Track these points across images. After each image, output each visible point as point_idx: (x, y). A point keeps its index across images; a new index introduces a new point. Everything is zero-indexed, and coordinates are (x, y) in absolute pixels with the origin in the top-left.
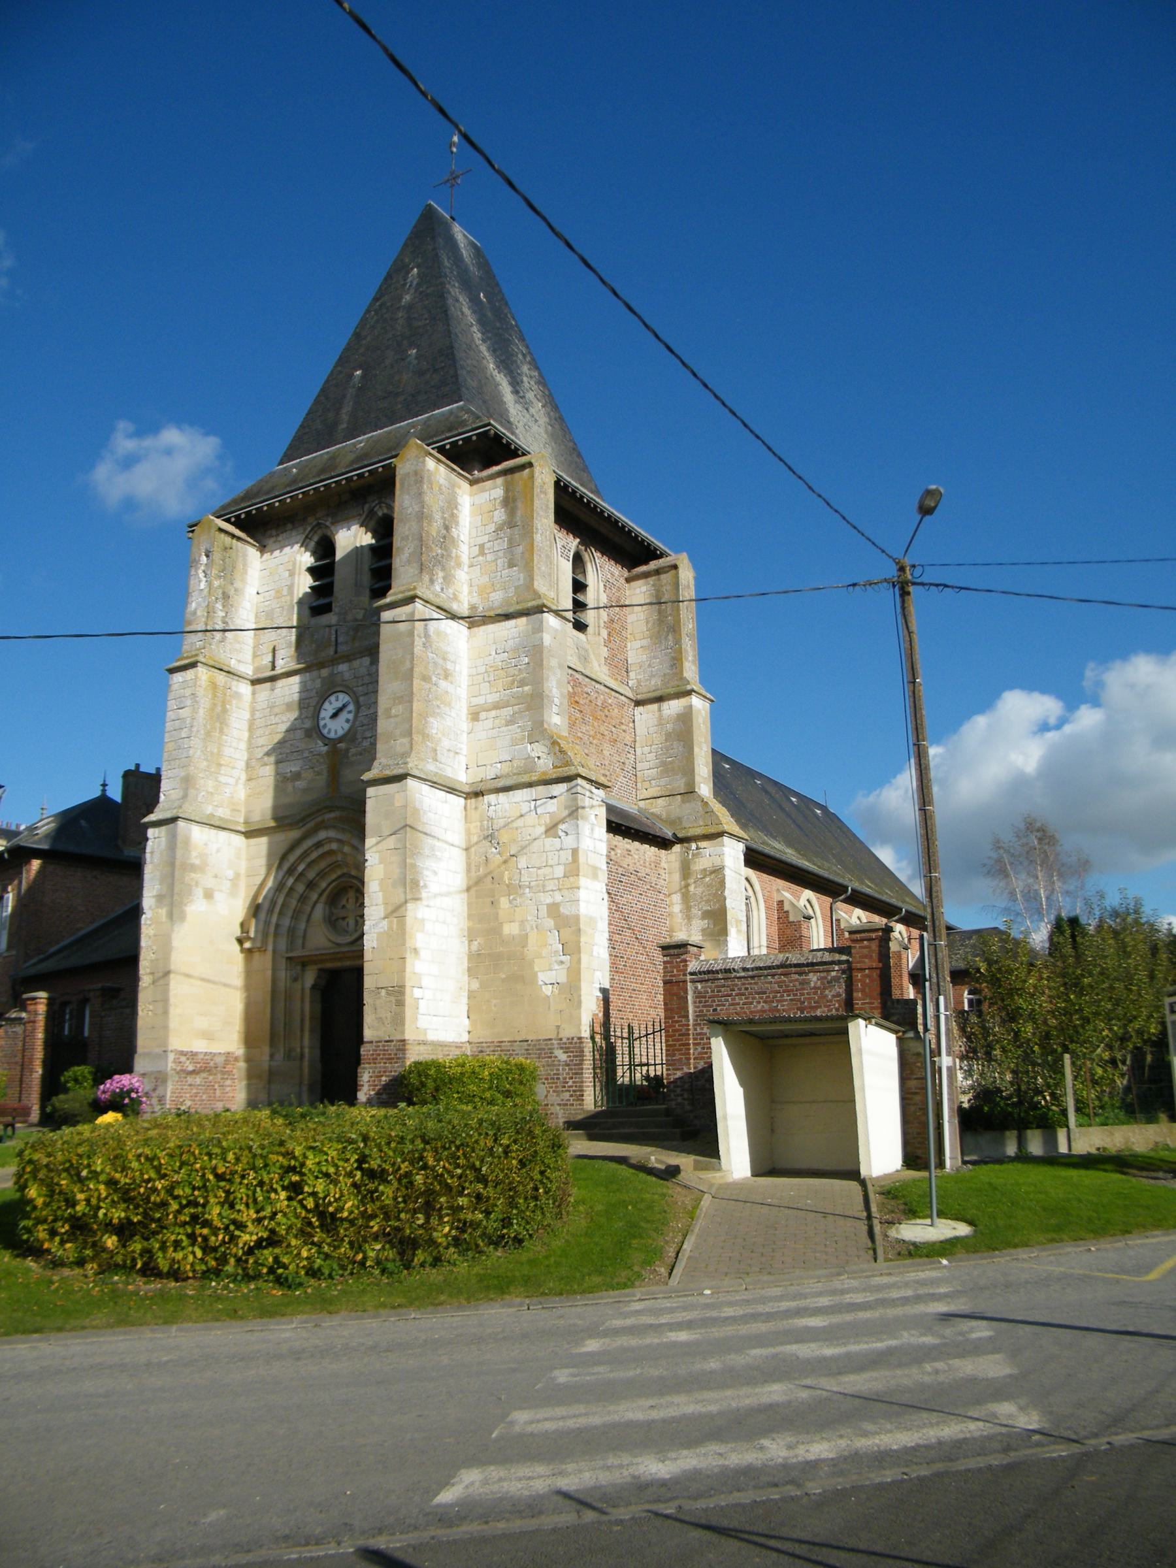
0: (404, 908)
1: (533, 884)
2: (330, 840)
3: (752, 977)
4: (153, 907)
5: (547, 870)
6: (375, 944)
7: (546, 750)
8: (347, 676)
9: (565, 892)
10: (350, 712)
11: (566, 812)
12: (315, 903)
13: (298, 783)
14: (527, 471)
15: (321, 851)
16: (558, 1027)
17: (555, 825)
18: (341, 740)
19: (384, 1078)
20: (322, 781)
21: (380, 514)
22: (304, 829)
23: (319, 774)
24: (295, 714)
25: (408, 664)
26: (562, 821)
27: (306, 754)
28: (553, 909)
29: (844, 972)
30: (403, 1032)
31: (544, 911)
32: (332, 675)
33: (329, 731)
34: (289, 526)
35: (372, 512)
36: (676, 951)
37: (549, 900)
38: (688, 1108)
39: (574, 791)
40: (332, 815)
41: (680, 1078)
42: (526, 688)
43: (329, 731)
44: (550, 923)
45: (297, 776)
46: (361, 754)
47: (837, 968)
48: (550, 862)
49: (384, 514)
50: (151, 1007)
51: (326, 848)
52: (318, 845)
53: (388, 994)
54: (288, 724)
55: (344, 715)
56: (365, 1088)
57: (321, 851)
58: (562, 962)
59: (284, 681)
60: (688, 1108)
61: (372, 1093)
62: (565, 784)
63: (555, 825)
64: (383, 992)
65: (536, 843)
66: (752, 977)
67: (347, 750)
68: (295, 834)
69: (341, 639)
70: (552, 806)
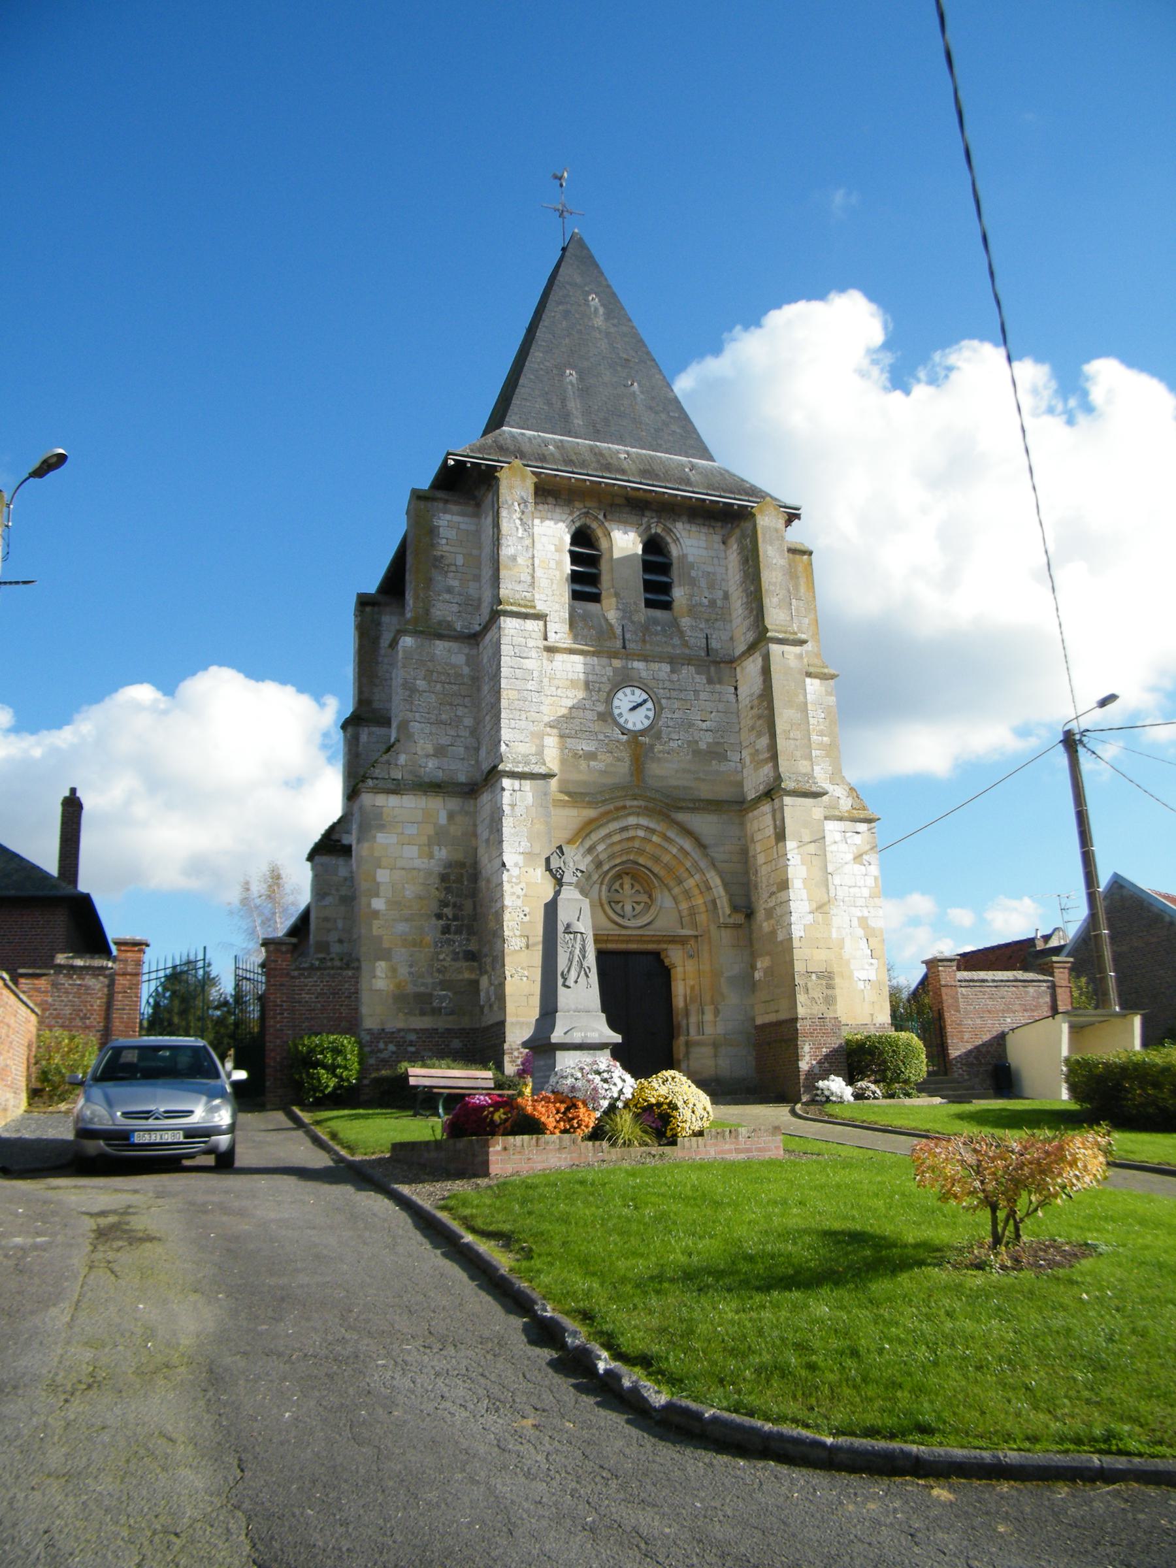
0: (827, 906)
1: (846, 899)
2: (638, 826)
3: (996, 987)
4: (521, 865)
5: (856, 890)
6: (802, 934)
7: (845, 793)
8: (644, 674)
9: (871, 909)
10: (649, 709)
11: (868, 847)
12: (595, 883)
13: (592, 763)
14: (805, 557)
15: (625, 835)
16: (872, 1015)
17: (861, 855)
18: (643, 733)
19: (824, 1050)
20: (624, 768)
21: (653, 531)
22: (602, 810)
23: (618, 759)
24: (581, 694)
25: (801, 698)
26: (866, 853)
27: (601, 737)
28: (863, 921)
29: (1048, 987)
30: (835, 1011)
31: (855, 923)
32: (625, 668)
33: (634, 724)
34: (550, 500)
35: (649, 528)
36: (949, 963)
37: (860, 914)
38: (966, 1077)
39: (873, 831)
40: (635, 803)
41: (959, 1056)
42: (825, 739)
43: (634, 724)
44: (860, 932)
45: (591, 756)
46: (669, 753)
47: (1045, 984)
48: (858, 884)
49: (656, 533)
50: (526, 973)
51: (631, 833)
52: (624, 829)
53: (818, 977)
54: (575, 701)
55: (642, 711)
56: (807, 1058)
57: (625, 835)
58: (872, 964)
59: (565, 657)
60: (966, 1077)
61: (814, 1062)
62: (866, 825)
63: (861, 855)
64: (814, 977)
65: (847, 866)
66: (996, 987)
67: (652, 746)
68: (591, 813)
69: (628, 636)
70: (858, 839)
